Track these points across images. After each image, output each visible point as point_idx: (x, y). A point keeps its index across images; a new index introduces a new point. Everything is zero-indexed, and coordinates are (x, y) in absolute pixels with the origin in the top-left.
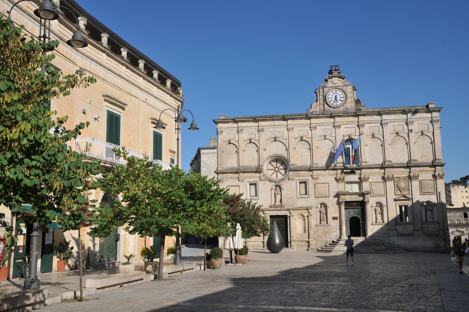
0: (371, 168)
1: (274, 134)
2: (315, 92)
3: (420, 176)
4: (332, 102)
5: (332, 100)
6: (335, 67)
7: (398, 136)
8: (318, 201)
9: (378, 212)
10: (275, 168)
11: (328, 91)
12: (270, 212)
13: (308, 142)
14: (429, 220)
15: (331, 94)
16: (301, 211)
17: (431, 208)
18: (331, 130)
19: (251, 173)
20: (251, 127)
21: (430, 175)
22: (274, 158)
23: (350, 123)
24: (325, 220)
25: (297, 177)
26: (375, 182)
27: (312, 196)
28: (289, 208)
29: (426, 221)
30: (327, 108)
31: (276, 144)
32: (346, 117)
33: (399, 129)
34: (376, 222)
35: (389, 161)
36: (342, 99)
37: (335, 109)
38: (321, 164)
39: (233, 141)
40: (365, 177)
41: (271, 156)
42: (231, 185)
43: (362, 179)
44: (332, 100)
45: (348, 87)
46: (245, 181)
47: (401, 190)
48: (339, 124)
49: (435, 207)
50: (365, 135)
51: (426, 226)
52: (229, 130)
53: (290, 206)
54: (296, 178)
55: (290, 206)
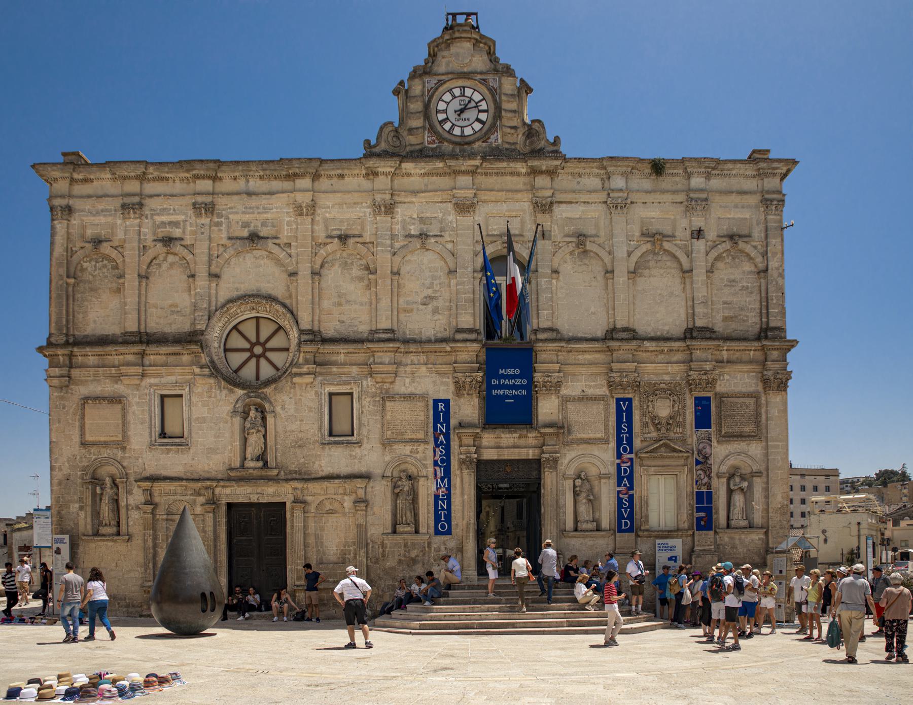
2: (396, 92)
3: (719, 383)
4: (447, 126)
6: (465, 16)
8: (387, 458)
9: (583, 495)
11: (437, 89)
14: (738, 519)
15: (447, 98)
17: (745, 484)
18: (442, 221)
19: (164, 358)
21: (747, 381)
25: (321, 374)
28: (289, 477)
29: (728, 526)
30: (430, 146)
32: (491, 174)
34: (576, 530)
35: (625, 330)
36: (483, 116)
38: (404, 333)
39: (105, 244)
43: (536, 386)
44: (447, 119)
46: (143, 384)
47: (659, 426)
53: (296, 472)
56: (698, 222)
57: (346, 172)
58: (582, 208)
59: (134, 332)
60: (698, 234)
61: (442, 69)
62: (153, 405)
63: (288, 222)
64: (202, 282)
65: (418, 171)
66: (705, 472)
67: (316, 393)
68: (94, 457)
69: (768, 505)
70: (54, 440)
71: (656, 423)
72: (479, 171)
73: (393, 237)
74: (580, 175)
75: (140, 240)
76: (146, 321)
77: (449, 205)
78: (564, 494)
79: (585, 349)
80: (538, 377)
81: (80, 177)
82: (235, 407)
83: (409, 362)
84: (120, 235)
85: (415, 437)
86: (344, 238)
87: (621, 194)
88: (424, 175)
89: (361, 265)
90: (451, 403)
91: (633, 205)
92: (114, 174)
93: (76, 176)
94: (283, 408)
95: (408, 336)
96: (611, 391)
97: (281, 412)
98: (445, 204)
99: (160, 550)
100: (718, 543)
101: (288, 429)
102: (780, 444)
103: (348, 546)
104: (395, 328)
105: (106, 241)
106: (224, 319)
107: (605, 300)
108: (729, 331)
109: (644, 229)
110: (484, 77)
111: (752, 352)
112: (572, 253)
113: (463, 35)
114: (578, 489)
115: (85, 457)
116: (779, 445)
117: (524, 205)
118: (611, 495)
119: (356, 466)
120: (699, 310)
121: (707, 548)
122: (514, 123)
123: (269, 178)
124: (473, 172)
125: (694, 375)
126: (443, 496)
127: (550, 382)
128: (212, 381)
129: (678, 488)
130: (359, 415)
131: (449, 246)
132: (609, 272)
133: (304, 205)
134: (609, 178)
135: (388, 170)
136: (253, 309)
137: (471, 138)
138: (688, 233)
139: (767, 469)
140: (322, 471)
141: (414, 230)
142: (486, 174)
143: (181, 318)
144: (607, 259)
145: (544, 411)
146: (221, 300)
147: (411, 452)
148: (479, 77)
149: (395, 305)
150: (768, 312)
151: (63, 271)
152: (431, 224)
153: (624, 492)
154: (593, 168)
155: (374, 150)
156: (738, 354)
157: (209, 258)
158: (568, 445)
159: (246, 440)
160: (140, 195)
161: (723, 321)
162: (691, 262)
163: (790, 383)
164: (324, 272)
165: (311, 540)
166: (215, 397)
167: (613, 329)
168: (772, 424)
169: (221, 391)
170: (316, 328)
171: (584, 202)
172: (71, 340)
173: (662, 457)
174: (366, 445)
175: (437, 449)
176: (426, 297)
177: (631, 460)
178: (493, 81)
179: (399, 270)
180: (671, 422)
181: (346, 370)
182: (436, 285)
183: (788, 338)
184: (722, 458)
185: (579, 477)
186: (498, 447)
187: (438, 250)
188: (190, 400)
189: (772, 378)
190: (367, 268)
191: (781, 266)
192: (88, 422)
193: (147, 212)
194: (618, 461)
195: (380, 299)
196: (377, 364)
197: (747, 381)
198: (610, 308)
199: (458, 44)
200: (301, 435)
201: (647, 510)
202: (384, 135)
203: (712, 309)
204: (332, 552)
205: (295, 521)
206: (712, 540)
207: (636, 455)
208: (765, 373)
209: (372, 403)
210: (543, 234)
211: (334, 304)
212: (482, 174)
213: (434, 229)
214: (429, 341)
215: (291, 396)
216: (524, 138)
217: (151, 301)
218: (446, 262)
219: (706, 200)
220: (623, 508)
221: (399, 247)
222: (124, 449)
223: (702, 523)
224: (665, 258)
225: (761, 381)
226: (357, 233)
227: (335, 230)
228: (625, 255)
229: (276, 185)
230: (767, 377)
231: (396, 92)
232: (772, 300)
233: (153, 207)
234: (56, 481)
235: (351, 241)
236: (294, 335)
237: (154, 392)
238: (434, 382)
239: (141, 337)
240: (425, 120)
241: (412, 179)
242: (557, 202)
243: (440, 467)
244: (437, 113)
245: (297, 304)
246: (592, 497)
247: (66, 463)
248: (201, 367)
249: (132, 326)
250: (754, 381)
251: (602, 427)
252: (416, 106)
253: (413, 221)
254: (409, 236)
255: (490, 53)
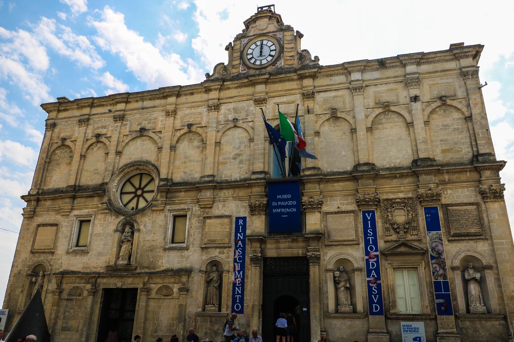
0: (328, 181)
1: (138, 125)
2: (227, 49)
3: (443, 196)
4: (252, 61)
5: (253, 57)
7: (389, 111)
8: (204, 258)
9: (342, 284)
10: (137, 190)
11: (247, 43)
12: (105, 280)
13: (200, 135)
14: (478, 307)
15: (253, 46)
16: (167, 280)
17: (478, 276)
20: (103, 115)
21: (467, 193)
22: (135, 168)
23: (284, 93)
24: (215, 302)
25: (169, 204)
26: (336, 213)
27: (193, 244)
29: (468, 311)
31: (141, 142)
32: (276, 82)
33: (386, 97)
34: (337, 311)
36: (273, 53)
37: (258, 72)
38: (221, 177)
39: (68, 140)
40: (310, 200)
41: (127, 165)
42: (44, 223)
43: (304, 205)
44: (253, 57)
45: (286, 33)
47: (398, 230)
48: (263, 95)
49: (489, 271)
50: (315, 113)
51: (468, 323)
52: (66, 122)
53: (147, 268)
54: (168, 207)
55: (147, 268)
56: (414, 92)
57: (194, 91)
58: (333, 94)
59: (71, 186)
60: (415, 99)
61: (251, 34)
62: (74, 226)
63: (161, 120)
64: (112, 156)
65: (234, 86)
66: (440, 265)
67: (165, 216)
68: (36, 259)
69: (502, 293)
70: (18, 249)
71: (395, 228)
72: (269, 81)
73: (218, 123)
74: (331, 75)
75: (85, 136)
76: (80, 179)
77: (252, 101)
78: (326, 283)
79: (339, 179)
80: (305, 199)
81: (63, 108)
82: (117, 227)
83: (223, 195)
84: (76, 135)
85: (222, 242)
86: (190, 126)
87: (358, 82)
88: (237, 88)
89: (199, 139)
90: (248, 219)
91: (368, 88)
92: (78, 105)
93: (61, 108)
94: (145, 226)
95: (223, 179)
96: (358, 206)
97: (143, 229)
98: (249, 101)
99: (59, 321)
100: (461, 326)
101: (146, 239)
102: (504, 241)
103: (173, 321)
104: (215, 174)
105: (69, 139)
106: (121, 175)
107: (352, 147)
108: (447, 159)
109: (377, 100)
110: (274, 34)
111: (468, 174)
112: (328, 120)
113: (262, 15)
114: (337, 279)
115: (32, 259)
116: (503, 243)
117: (297, 98)
118: (364, 284)
119: (184, 263)
120: (421, 147)
121: (450, 331)
122: (292, 54)
123: (154, 99)
124: (266, 82)
125: (422, 191)
126: (239, 284)
127: (313, 202)
128: (107, 211)
129: (419, 279)
130: (189, 229)
131: (251, 124)
132: (353, 131)
133: (170, 111)
134: (350, 74)
135: (217, 87)
136: (138, 169)
137: (266, 65)
138: (408, 100)
139: (496, 262)
140: (163, 266)
141: (231, 117)
142: (274, 83)
143: (98, 176)
144: (351, 121)
145: (310, 222)
146: (121, 165)
147: (219, 253)
148: (271, 35)
149: (216, 160)
150: (477, 144)
151: (44, 156)
152: (241, 113)
153: (373, 282)
154: (338, 70)
155: (210, 78)
156: (456, 175)
157: (118, 143)
158: (329, 246)
159: (120, 247)
160: (89, 115)
161: (441, 153)
162: (412, 117)
163: (505, 193)
164: (179, 145)
165: (150, 315)
166: (108, 221)
167: (358, 165)
168: (494, 226)
169: (112, 217)
170: (170, 177)
171: (335, 90)
172: (40, 192)
173: (402, 254)
174: (191, 249)
175: (236, 251)
176: (236, 155)
177: (377, 256)
178: (279, 35)
179: (220, 140)
180: (407, 227)
181: (184, 201)
182: (242, 147)
183: (498, 160)
184: (454, 254)
185: (339, 270)
186: (278, 248)
187: (244, 127)
188: (94, 223)
189: (488, 190)
190: (202, 141)
191: (482, 112)
192: (37, 238)
193: (91, 122)
194: (366, 257)
195: (207, 158)
196: (203, 196)
197: (467, 193)
198: (355, 151)
199: (261, 20)
200: (153, 243)
201: (394, 296)
202: (217, 70)
203: (432, 146)
204: (164, 325)
205: (141, 301)
206: (454, 323)
207: (382, 253)
208: (481, 186)
209: (197, 221)
210: (308, 112)
211: (182, 163)
212: (271, 83)
213: (242, 115)
214: (236, 181)
215: (150, 218)
216: (298, 61)
217: (85, 168)
218: (249, 133)
219: (418, 78)
220: (373, 294)
221: (221, 127)
222: (53, 253)
223: (443, 308)
224: (394, 116)
225: (479, 193)
226: (199, 122)
227: (187, 122)
228: (363, 117)
229: (157, 102)
230: (483, 189)
231: (227, 49)
232: (479, 135)
233: (95, 120)
234: (13, 274)
235: (195, 127)
236: (157, 182)
237: (76, 219)
238: (237, 206)
239: (75, 188)
240: (240, 60)
241: (231, 90)
242: (317, 92)
243: (238, 263)
244: (247, 55)
245: (160, 163)
246: (348, 285)
247: (21, 263)
248: (102, 203)
249: (72, 183)
250: (474, 193)
251: (353, 233)
252: (237, 55)
253: (231, 113)
254: (228, 121)
255: (279, 22)
